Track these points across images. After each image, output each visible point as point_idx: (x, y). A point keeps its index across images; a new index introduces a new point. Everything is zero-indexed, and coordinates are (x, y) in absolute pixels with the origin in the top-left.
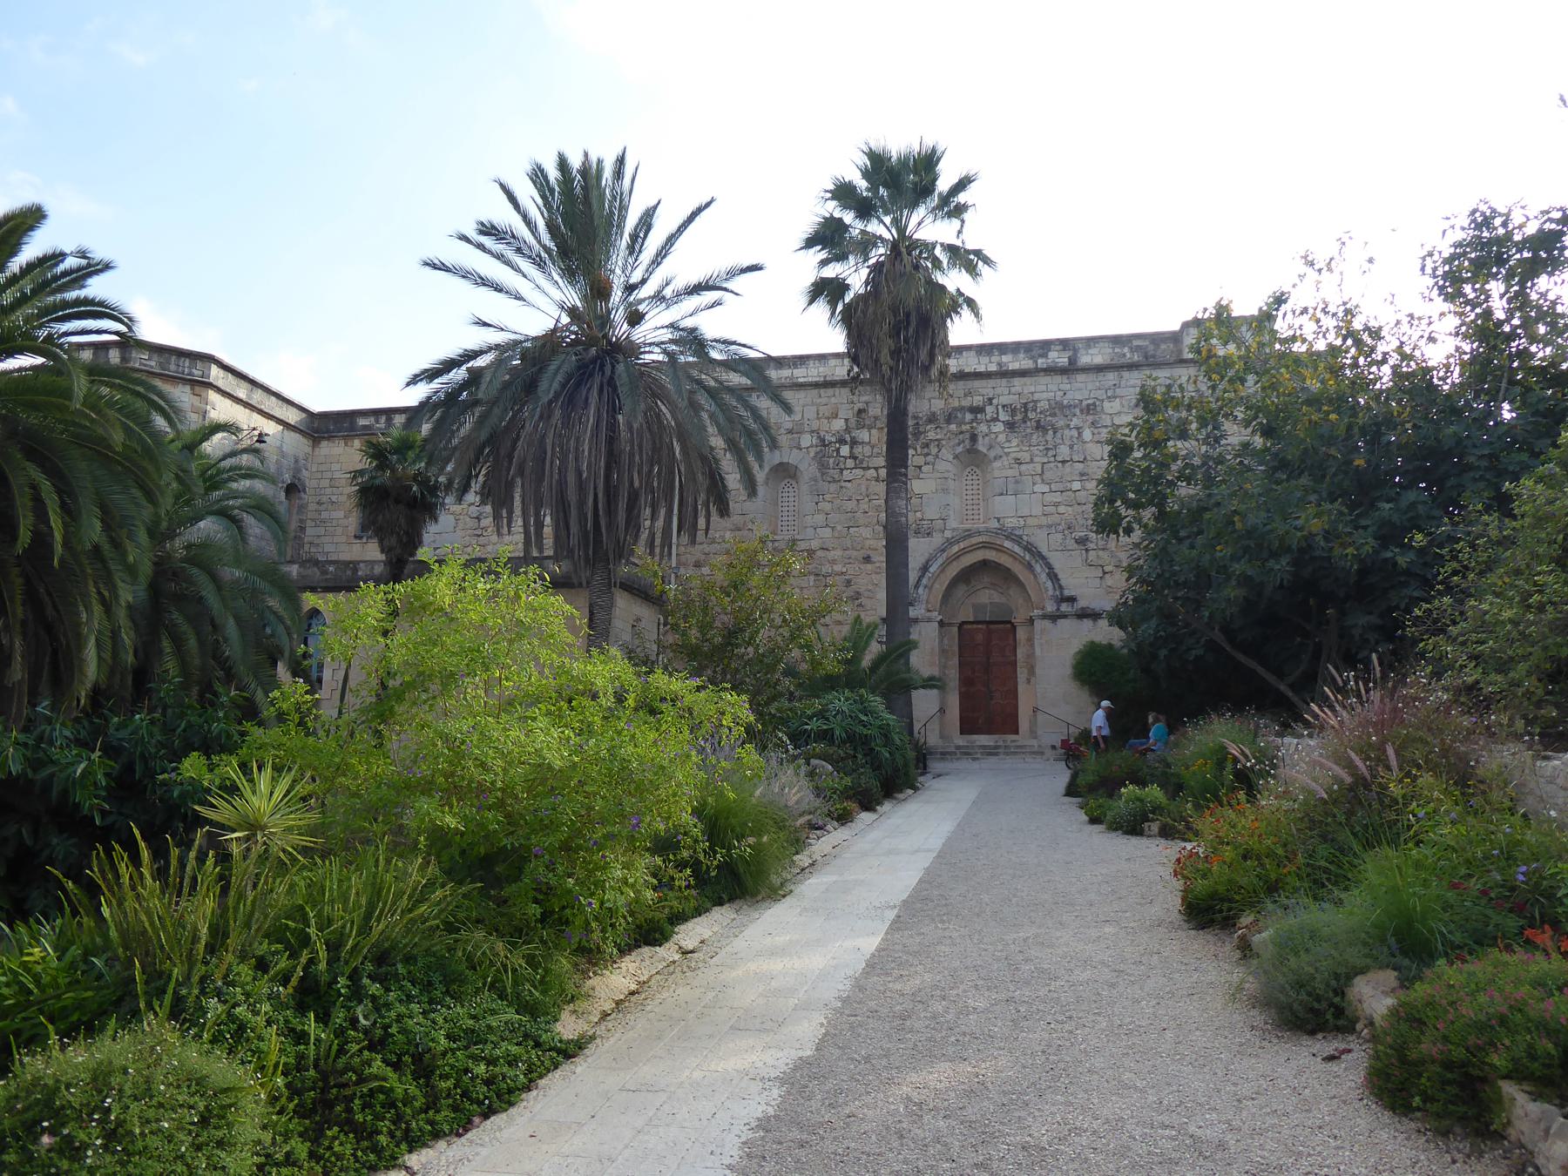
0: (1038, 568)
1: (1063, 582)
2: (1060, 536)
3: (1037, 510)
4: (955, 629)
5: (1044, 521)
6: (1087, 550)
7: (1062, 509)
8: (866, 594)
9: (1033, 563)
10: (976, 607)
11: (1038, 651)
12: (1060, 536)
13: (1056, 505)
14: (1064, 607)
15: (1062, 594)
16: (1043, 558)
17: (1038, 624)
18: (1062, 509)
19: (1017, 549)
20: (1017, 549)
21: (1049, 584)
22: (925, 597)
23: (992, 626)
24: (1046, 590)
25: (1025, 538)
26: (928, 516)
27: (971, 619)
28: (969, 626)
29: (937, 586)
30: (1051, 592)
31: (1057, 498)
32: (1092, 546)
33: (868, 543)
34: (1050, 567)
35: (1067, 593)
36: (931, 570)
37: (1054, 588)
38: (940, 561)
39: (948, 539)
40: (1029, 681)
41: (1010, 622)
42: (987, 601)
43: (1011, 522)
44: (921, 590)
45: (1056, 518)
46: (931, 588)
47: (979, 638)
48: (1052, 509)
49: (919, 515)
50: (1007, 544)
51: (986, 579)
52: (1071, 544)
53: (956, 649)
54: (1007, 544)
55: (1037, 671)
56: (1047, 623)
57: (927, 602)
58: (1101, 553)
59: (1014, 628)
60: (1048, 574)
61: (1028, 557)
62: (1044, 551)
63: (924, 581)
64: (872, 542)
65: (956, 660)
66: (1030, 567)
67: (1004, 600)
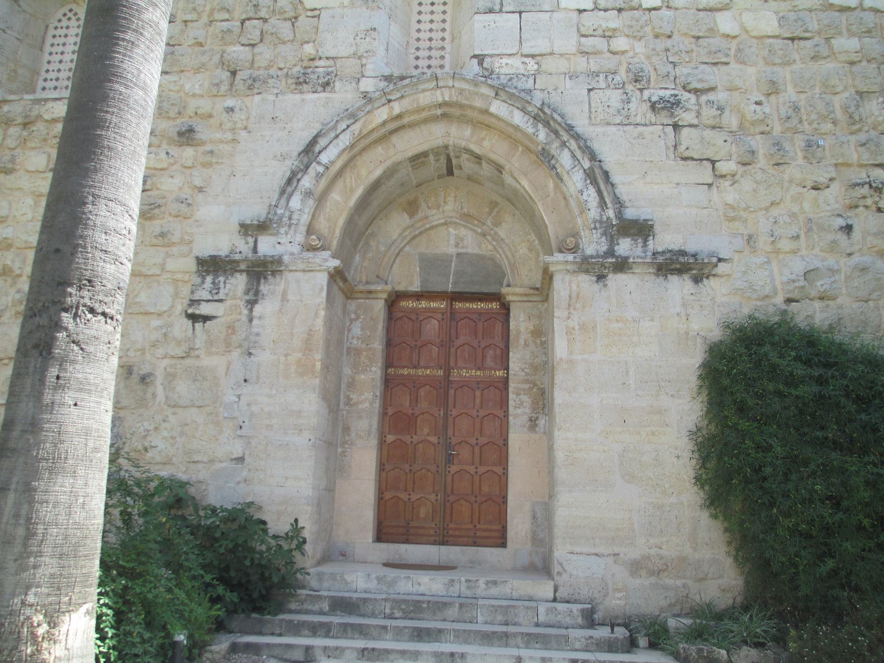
0: (565, 159)
1: (623, 191)
2: (615, 97)
3: (568, 43)
4: (379, 306)
5: (581, 64)
6: (676, 127)
7: (620, 43)
8: (174, 207)
9: (554, 148)
10: (430, 263)
11: (560, 348)
12: (615, 97)
13: (608, 35)
14: (624, 247)
15: (619, 214)
16: (577, 137)
17: (562, 286)
18: (620, 43)
19: (518, 118)
20: (518, 118)
21: (591, 195)
22: (305, 218)
23: (458, 305)
24: (583, 209)
25: (538, 98)
26: (328, 50)
27: (416, 287)
28: (411, 304)
29: (335, 196)
30: (594, 213)
31: (612, 21)
32: (688, 117)
33: (193, 104)
34: (593, 157)
35: (630, 213)
36: (324, 158)
37: (603, 204)
38: (345, 140)
39: (365, 95)
40: (533, 423)
41: (496, 297)
42: (452, 250)
43: (507, 67)
44: (295, 202)
45: (609, 62)
46: (321, 200)
47: (432, 327)
48: (599, 43)
49: (309, 49)
50: (498, 108)
51: (450, 207)
52: (639, 110)
53: (378, 345)
54: (498, 108)
55: (559, 397)
56: (585, 282)
57: (310, 231)
58: (708, 133)
59: (506, 308)
60: (590, 176)
61: (542, 134)
62: (581, 124)
63: (307, 182)
64: (202, 102)
65: (375, 372)
66: (546, 158)
67: (486, 248)
